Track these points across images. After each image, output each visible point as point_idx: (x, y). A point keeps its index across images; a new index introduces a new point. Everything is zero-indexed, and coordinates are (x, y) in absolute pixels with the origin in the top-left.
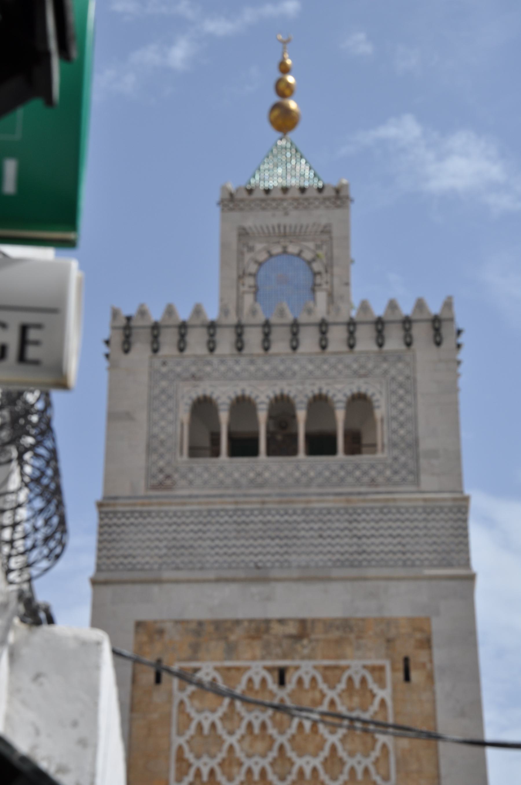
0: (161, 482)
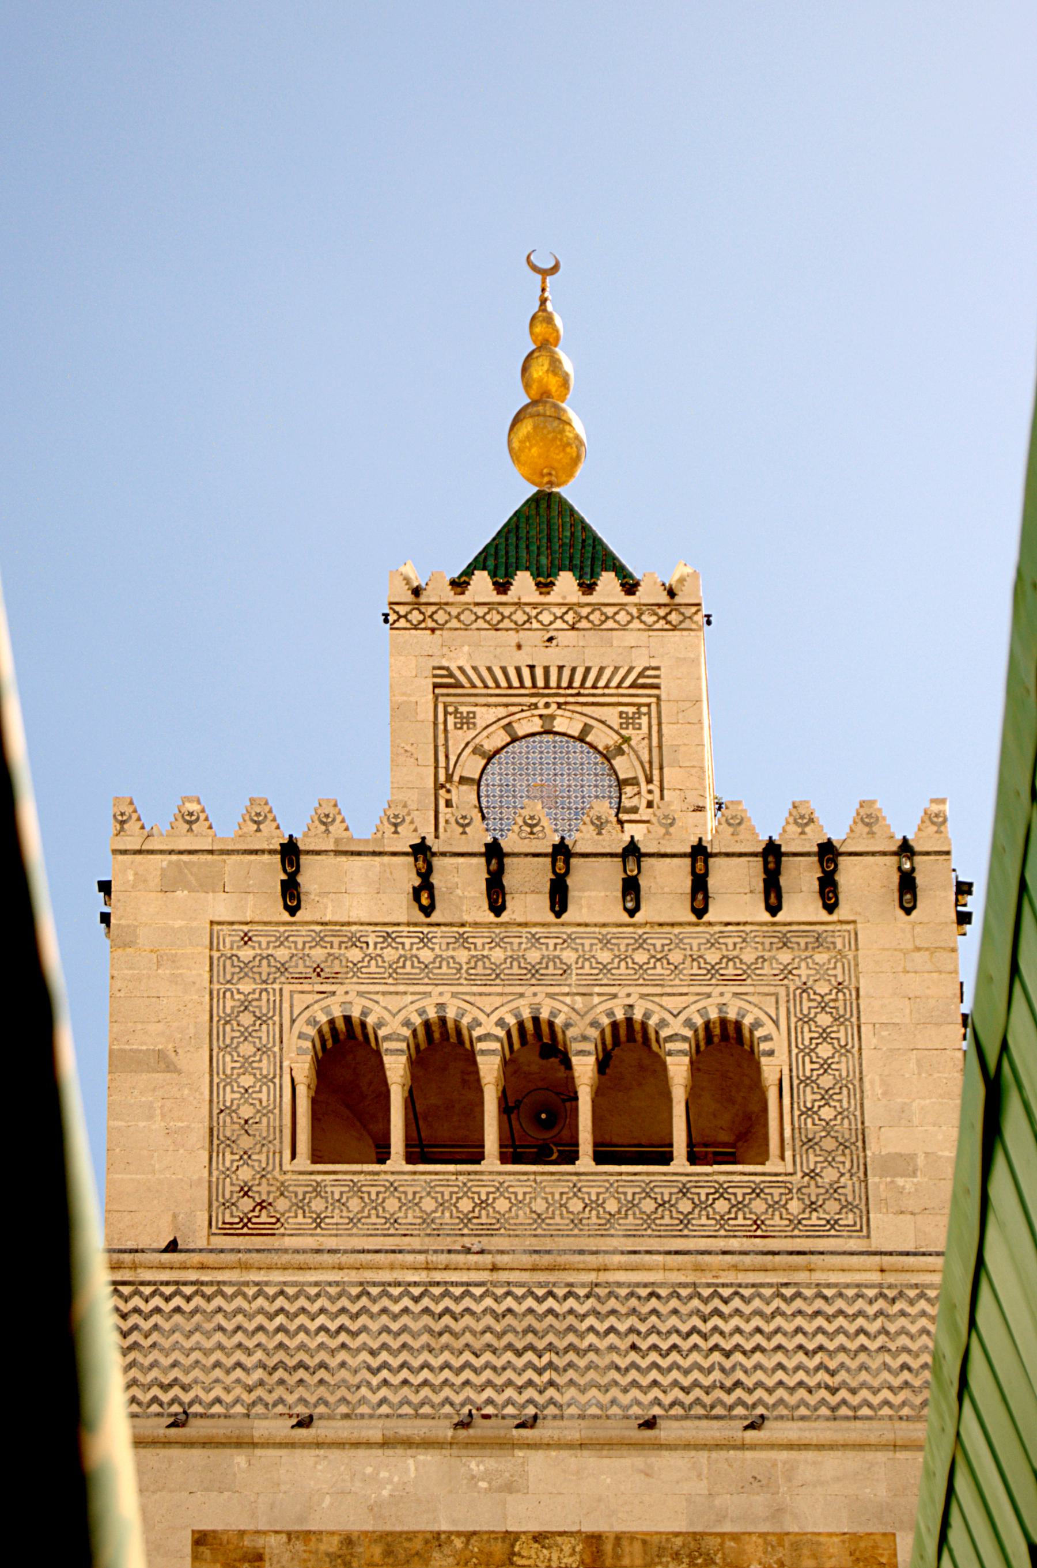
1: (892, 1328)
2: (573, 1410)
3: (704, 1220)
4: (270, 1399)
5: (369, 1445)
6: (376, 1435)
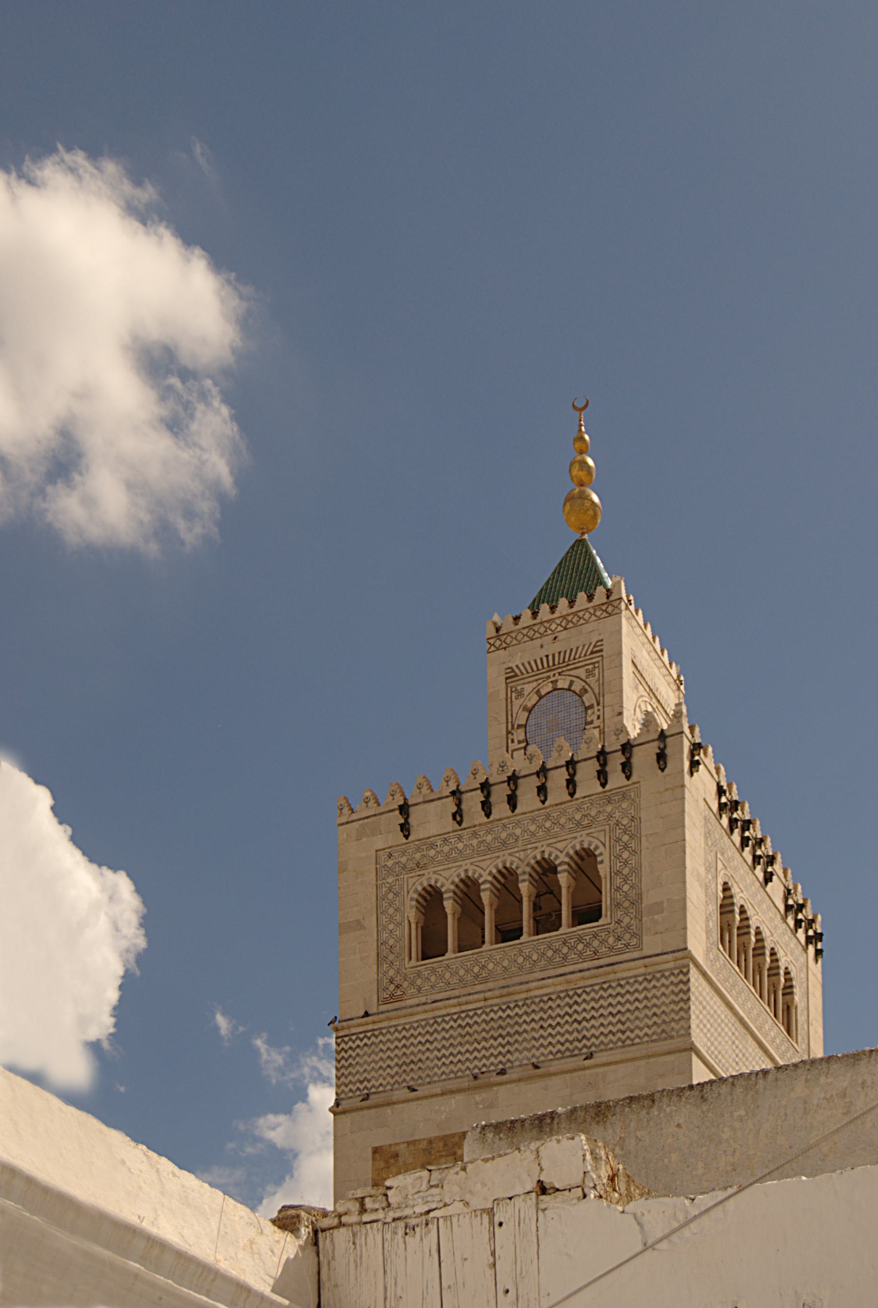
0: (391, 994)
1: (649, 995)
2: (517, 1063)
3: (573, 956)
4: (400, 1080)
5: (437, 1095)
6: (438, 1091)
